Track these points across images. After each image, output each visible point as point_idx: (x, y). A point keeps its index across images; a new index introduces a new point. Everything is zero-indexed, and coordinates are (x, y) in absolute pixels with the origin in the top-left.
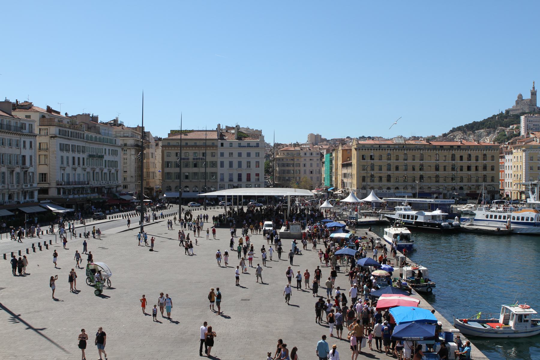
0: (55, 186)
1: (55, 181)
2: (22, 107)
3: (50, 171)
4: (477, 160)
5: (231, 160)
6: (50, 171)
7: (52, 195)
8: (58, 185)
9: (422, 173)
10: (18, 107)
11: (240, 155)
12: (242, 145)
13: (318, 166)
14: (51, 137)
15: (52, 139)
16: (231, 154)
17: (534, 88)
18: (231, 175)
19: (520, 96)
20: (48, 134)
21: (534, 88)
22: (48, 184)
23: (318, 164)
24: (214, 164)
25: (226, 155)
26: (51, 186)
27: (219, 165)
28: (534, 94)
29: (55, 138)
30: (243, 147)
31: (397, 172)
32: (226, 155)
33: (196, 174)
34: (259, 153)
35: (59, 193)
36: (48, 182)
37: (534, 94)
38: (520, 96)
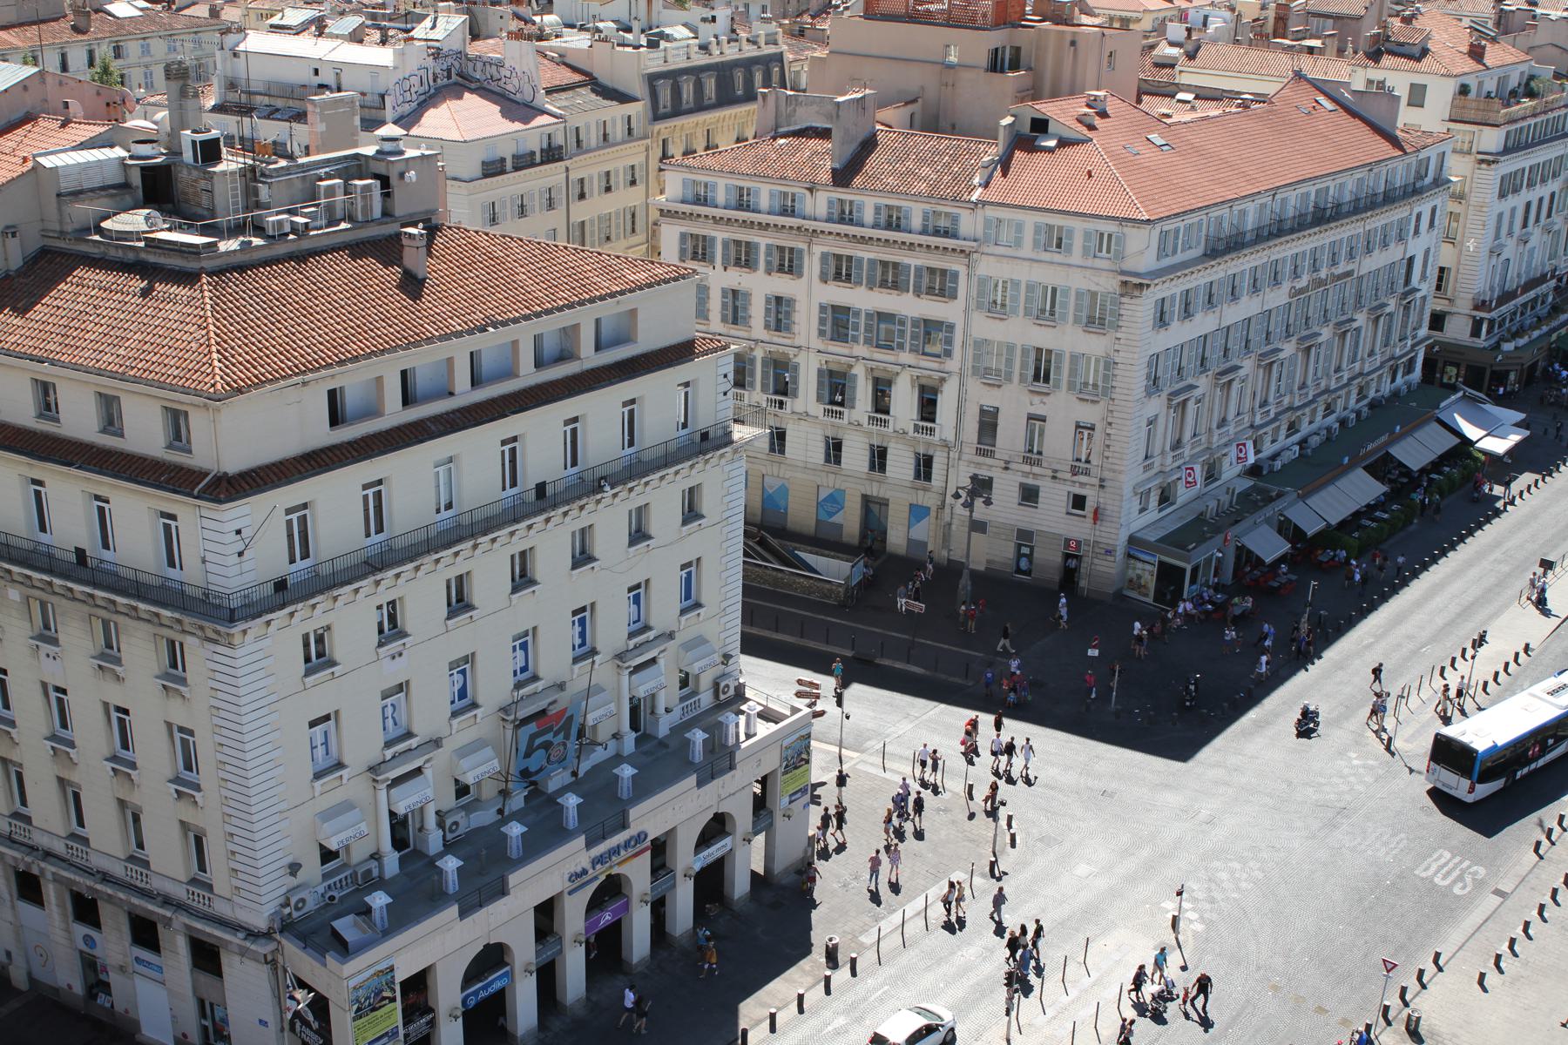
0: (1468, 312)
1: (1471, 296)
2: (1401, 50)
3: (1459, 263)
6: (1459, 263)
7: (1455, 336)
8: (1476, 308)
10: (1387, 45)
14: (1482, 161)
15: (1484, 166)
20: (1474, 150)
22: (1447, 302)
26: (1454, 310)
29: (1493, 166)
35: (1476, 332)
36: (1449, 294)
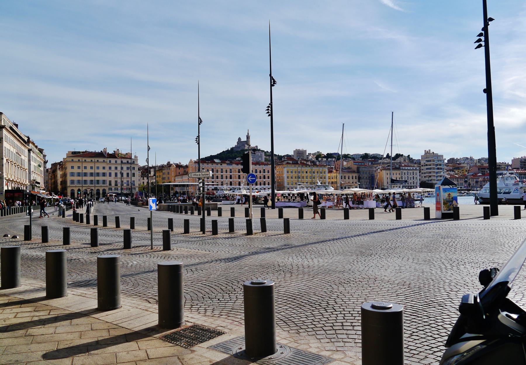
4: (260, 172)
5: (116, 172)
9: (231, 180)
11: (122, 168)
12: (123, 162)
13: (139, 180)
16: (116, 168)
17: (248, 134)
18: (116, 182)
19: (239, 139)
21: (248, 134)
23: (139, 179)
24: (104, 174)
25: (113, 168)
27: (108, 175)
28: (248, 137)
30: (124, 163)
31: (217, 180)
32: (113, 168)
33: (91, 181)
34: (134, 167)
37: (248, 137)
38: (239, 139)
